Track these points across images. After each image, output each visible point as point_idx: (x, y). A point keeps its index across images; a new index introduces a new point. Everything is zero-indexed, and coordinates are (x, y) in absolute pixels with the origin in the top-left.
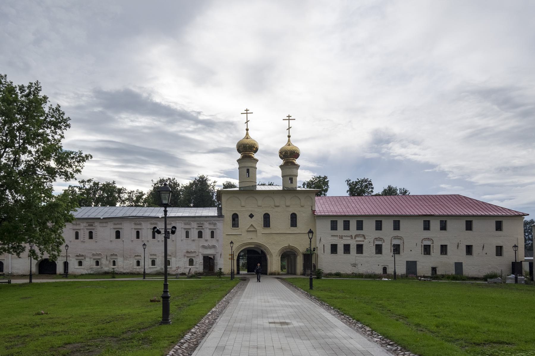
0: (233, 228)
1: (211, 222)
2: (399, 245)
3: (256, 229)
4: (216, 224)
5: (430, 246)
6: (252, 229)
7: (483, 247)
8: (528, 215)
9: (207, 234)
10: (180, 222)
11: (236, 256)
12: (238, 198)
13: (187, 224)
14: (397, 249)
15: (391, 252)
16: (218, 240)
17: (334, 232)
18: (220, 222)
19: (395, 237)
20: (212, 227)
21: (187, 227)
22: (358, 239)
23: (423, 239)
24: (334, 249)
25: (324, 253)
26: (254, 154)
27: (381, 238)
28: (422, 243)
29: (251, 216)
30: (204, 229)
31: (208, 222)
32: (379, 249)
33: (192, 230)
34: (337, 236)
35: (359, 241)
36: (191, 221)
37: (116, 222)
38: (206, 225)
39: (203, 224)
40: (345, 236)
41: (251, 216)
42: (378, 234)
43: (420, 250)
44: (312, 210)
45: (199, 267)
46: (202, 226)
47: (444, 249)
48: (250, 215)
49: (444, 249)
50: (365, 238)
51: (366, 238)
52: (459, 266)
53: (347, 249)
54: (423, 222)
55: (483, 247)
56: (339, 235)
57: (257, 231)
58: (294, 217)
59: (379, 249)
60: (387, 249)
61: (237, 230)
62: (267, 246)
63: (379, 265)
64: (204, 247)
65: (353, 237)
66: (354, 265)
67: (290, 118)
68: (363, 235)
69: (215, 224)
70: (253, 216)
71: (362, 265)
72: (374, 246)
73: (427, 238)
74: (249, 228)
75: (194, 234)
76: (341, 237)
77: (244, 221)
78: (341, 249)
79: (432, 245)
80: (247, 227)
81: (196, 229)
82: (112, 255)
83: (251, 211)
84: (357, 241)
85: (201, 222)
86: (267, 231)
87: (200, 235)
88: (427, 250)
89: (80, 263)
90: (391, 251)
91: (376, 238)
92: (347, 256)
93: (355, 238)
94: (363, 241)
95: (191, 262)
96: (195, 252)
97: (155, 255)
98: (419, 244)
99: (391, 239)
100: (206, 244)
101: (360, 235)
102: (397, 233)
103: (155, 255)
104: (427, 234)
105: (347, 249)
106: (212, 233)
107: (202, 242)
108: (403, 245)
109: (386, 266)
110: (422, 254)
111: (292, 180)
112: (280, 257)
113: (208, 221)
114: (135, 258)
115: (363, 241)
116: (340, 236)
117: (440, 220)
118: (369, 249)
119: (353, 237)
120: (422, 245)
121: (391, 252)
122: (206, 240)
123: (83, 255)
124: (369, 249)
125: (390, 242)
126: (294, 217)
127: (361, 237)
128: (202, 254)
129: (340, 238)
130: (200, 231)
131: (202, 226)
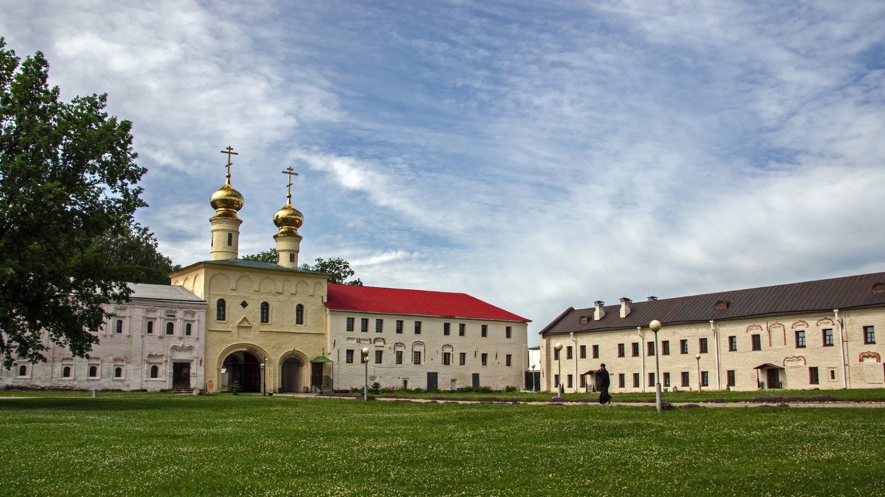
0: (218, 321)
1: (188, 310)
2: (420, 353)
3: (250, 324)
5: (449, 354)
6: (246, 324)
7: (496, 356)
8: (531, 321)
9: (179, 328)
10: (141, 307)
12: (305, 282)
13: (152, 311)
14: (417, 358)
15: (412, 361)
17: (350, 334)
18: (201, 310)
20: (189, 317)
21: (151, 315)
22: (378, 344)
26: (235, 211)
28: (442, 350)
29: (244, 305)
30: (177, 320)
32: (399, 358)
33: (158, 320)
34: (354, 339)
35: (379, 346)
36: (158, 307)
38: (180, 314)
39: (175, 312)
40: (362, 339)
41: (244, 305)
42: (398, 338)
43: (440, 359)
45: (165, 380)
46: (174, 316)
48: (242, 303)
51: (386, 342)
52: (476, 377)
54: (396, 323)
55: (496, 356)
56: (355, 337)
57: (251, 327)
58: (300, 309)
59: (399, 358)
60: (408, 357)
61: (223, 325)
62: (266, 351)
63: (399, 378)
64: (175, 348)
65: (372, 342)
68: (383, 339)
69: (193, 314)
71: (381, 377)
73: (447, 345)
74: (241, 323)
75: (159, 327)
77: (234, 313)
79: (451, 353)
80: (238, 321)
81: (166, 319)
84: (376, 346)
85: (174, 310)
86: (265, 328)
87: (170, 329)
91: (396, 343)
93: (374, 343)
94: (383, 347)
95: (154, 372)
96: (161, 356)
97: (98, 359)
98: (440, 352)
100: (180, 344)
101: (379, 338)
103: (98, 359)
104: (447, 340)
106: (189, 327)
108: (425, 352)
113: (183, 308)
114: (63, 363)
115: (383, 347)
116: (357, 339)
117: (505, 326)
118: (389, 357)
119: (372, 342)
122: (180, 338)
124: (389, 357)
125: (411, 348)
126: (300, 309)
127: (381, 341)
128: (172, 360)
129: (357, 342)
130: (170, 323)
131: (174, 316)
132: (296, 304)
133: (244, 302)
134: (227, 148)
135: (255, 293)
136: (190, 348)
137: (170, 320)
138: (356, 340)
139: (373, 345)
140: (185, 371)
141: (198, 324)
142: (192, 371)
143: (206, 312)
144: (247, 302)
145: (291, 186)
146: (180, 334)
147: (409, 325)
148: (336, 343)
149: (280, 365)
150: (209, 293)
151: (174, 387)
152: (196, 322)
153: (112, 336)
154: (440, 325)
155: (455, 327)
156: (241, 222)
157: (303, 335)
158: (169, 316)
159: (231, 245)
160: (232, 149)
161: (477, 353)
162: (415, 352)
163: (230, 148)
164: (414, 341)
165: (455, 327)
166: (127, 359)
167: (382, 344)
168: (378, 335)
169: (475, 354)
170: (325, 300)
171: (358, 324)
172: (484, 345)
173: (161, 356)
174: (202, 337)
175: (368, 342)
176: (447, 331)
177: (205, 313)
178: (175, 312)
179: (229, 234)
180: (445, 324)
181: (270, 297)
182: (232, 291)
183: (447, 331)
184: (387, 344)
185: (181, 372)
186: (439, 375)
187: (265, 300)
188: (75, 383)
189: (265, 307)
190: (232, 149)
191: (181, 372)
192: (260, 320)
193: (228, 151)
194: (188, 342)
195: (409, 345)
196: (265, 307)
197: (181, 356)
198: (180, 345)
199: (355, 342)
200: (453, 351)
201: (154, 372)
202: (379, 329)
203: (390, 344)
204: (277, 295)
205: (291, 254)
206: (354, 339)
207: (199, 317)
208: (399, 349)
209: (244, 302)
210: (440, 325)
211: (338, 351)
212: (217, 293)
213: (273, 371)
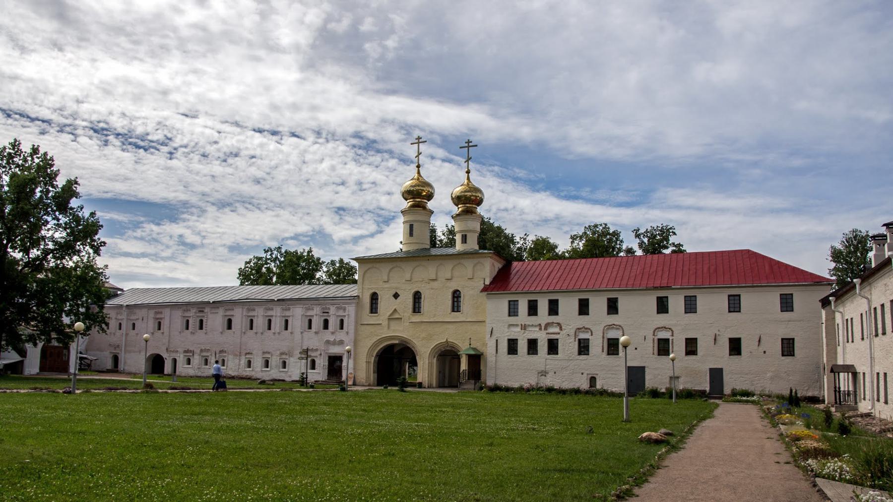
0: (370, 315)
5: (667, 340)
6: (397, 316)
7: (759, 341)
9: (333, 323)
14: (613, 347)
15: (603, 351)
16: (347, 333)
17: (513, 320)
19: (610, 326)
20: (341, 313)
22: (551, 330)
23: (656, 329)
27: (587, 329)
28: (654, 335)
31: (335, 306)
32: (584, 348)
34: (517, 325)
37: (227, 308)
38: (332, 310)
40: (529, 325)
41: (396, 296)
42: (583, 321)
43: (650, 347)
46: (328, 313)
47: (691, 347)
49: (691, 347)
50: (561, 329)
51: (563, 328)
52: (716, 375)
53: (532, 345)
55: (759, 341)
56: (519, 323)
57: (401, 318)
58: (456, 296)
59: (584, 348)
60: (597, 345)
61: (375, 318)
63: (582, 374)
65: (543, 328)
66: (544, 373)
67: (470, 144)
68: (559, 324)
69: (345, 309)
71: (555, 373)
72: (575, 341)
73: (662, 328)
74: (391, 315)
75: (317, 323)
76: (524, 327)
78: (523, 346)
79: (671, 338)
80: (389, 313)
83: (396, 288)
84: (548, 333)
86: (417, 318)
88: (663, 347)
89: (189, 362)
90: (603, 349)
91: (579, 329)
92: (533, 358)
93: (546, 329)
94: (559, 334)
96: (317, 350)
97: (269, 353)
98: (650, 337)
99: (604, 330)
100: (332, 339)
102: (613, 319)
103: (269, 353)
104: (662, 320)
105: (532, 345)
107: (327, 336)
109: (594, 376)
110: (653, 354)
111: (466, 239)
115: (559, 334)
116: (522, 325)
118: (568, 346)
119: (543, 328)
121: (603, 351)
122: (333, 333)
123: (191, 351)
124: (568, 346)
125: (602, 334)
126: (456, 296)
127: (556, 327)
129: (522, 329)
131: (328, 313)
132: (451, 290)
133: (396, 293)
134: (466, 143)
136: (341, 343)
137: (325, 316)
138: (520, 327)
140: (338, 363)
142: (344, 364)
144: (399, 293)
148: (493, 332)
151: (328, 379)
153: (279, 333)
154: (720, 300)
155: (676, 302)
157: (457, 324)
158: (324, 313)
160: (471, 142)
161: (718, 338)
163: (469, 142)
165: (676, 302)
166: (290, 354)
167: (557, 330)
168: (553, 319)
169: (715, 340)
171: (523, 307)
172: (734, 325)
173: (317, 350)
174: (352, 332)
175: (537, 329)
176: (662, 306)
180: (658, 298)
182: (384, 284)
183: (662, 306)
184: (565, 329)
185: (335, 364)
187: (416, 290)
188: (253, 373)
189: (417, 296)
190: (471, 142)
191: (335, 364)
192: (411, 310)
193: (467, 145)
194: (341, 335)
195: (598, 331)
196: (417, 296)
197: (335, 350)
198: (332, 340)
199: (518, 329)
202: (553, 308)
203: (569, 329)
205: (462, 235)
206: (517, 325)
208: (583, 336)
209: (396, 293)
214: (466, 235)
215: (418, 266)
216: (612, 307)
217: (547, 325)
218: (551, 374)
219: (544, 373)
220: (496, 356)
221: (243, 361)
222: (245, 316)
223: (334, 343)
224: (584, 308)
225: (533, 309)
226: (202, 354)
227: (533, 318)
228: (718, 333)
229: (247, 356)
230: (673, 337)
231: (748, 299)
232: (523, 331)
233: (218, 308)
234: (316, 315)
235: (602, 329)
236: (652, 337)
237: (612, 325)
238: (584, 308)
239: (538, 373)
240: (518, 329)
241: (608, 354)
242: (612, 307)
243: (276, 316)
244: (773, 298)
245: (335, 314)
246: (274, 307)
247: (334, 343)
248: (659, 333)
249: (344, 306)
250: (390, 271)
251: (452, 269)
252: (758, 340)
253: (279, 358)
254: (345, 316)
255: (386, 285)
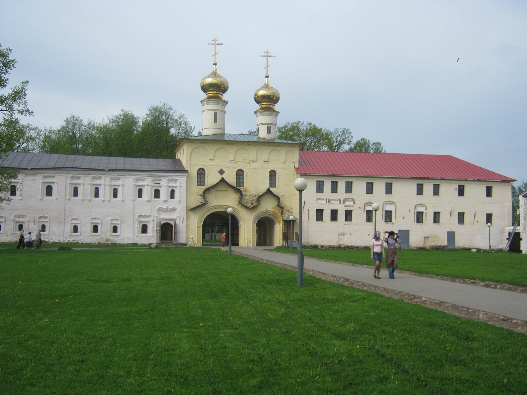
1: (171, 178)
2: (391, 212)
4: (177, 181)
5: (422, 213)
7: (475, 215)
8: (516, 181)
9: (164, 193)
11: (202, 221)
15: (383, 219)
17: (320, 195)
19: (387, 202)
22: (347, 203)
24: (320, 214)
25: (308, 220)
28: (415, 209)
32: (369, 216)
34: (323, 199)
35: (348, 206)
40: (332, 200)
43: (413, 217)
44: (294, 167)
46: (160, 184)
47: (437, 217)
49: (437, 217)
50: (355, 203)
52: (451, 236)
53: (334, 215)
55: (475, 215)
56: (325, 198)
63: (369, 235)
64: (160, 210)
66: (343, 234)
68: (353, 200)
70: (224, 172)
71: (350, 234)
72: (364, 212)
73: (420, 204)
75: (148, 193)
76: (328, 201)
78: (327, 215)
79: (425, 211)
81: (153, 186)
82: (40, 217)
83: (221, 166)
84: (346, 206)
85: (159, 178)
87: (157, 194)
88: (419, 217)
90: (383, 218)
92: (334, 223)
93: (344, 202)
94: (353, 206)
95: (144, 229)
96: (149, 216)
98: (413, 211)
99: (383, 204)
101: (349, 198)
102: (389, 198)
104: (420, 199)
105: (334, 215)
108: (396, 212)
110: (415, 222)
112: (256, 223)
113: (167, 177)
114: (72, 222)
115: (353, 206)
118: (359, 216)
120: (415, 212)
124: (359, 216)
127: (351, 201)
128: (158, 219)
129: (327, 202)
131: (160, 184)
135: (231, 161)
136: (173, 210)
138: (325, 201)
139: (342, 204)
141: (180, 189)
143: (187, 179)
144: (224, 170)
145: (266, 66)
146: (165, 198)
147: (379, 187)
149: (255, 222)
150: (190, 164)
152: (179, 188)
153: (109, 201)
155: (428, 188)
156: (227, 103)
159: (216, 122)
161: (452, 212)
162: (386, 211)
164: (384, 201)
165: (428, 188)
167: (351, 203)
168: (348, 195)
169: (451, 213)
170: (297, 166)
171: (327, 186)
173: (149, 216)
175: (338, 202)
176: (420, 191)
177: (186, 180)
178: (160, 180)
179: (214, 113)
181: (245, 165)
182: (210, 161)
183: (420, 191)
184: (357, 203)
186: (410, 232)
188: (81, 238)
194: (172, 204)
197: (166, 217)
198: (165, 208)
199: (324, 202)
200: (426, 209)
201: (144, 229)
202: (349, 188)
203: (360, 203)
204: (251, 163)
205: (268, 127)
206: (323, 199)
207: (180, 184)
210: (412, 187)
211: (308, 210)
212: (198, 163)
213: (247, 228)
214: (270, 127)
215: (241, 149)
216: (389, 190)
217: (345, 200)
218: (347, 235)
219: (343, 234)
220: (308, 222)
221: (69, 228)
222: (70, 183)
223: (166, 210)
224: (370, 189)
225: (334, 188)
226: (40, 220)
227: (334, 194)
228: (452, 209)
229: (73, 222)
230: (427, 211)
231: (468, 189)
232: (328, 204)
233: (35, 174)
234: (148, 185)
235: (382, 203)
236: (414, 210)
237: (388, 201)
238: (370, 189)
239: (339, 234)
240: (324, 202)
241: (385, 221)
242: (389, 190)
243: (105, 185)
244: (482, 189)
245: (167, 185)
246: (103, 176)
247: (166, 210)
248: (418, 208)
249: (176, 178)
250: (216, 151)
251: (269, 154)
252: (474, 214)
253: (110, 223)
254: (176, 187)
255: (213, 163)
